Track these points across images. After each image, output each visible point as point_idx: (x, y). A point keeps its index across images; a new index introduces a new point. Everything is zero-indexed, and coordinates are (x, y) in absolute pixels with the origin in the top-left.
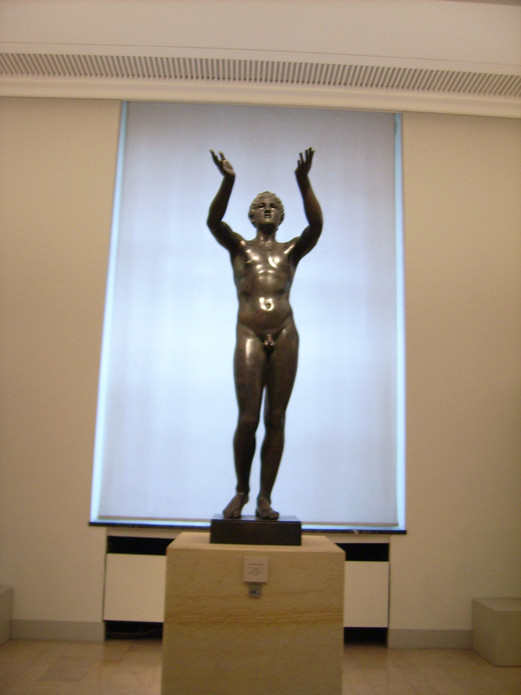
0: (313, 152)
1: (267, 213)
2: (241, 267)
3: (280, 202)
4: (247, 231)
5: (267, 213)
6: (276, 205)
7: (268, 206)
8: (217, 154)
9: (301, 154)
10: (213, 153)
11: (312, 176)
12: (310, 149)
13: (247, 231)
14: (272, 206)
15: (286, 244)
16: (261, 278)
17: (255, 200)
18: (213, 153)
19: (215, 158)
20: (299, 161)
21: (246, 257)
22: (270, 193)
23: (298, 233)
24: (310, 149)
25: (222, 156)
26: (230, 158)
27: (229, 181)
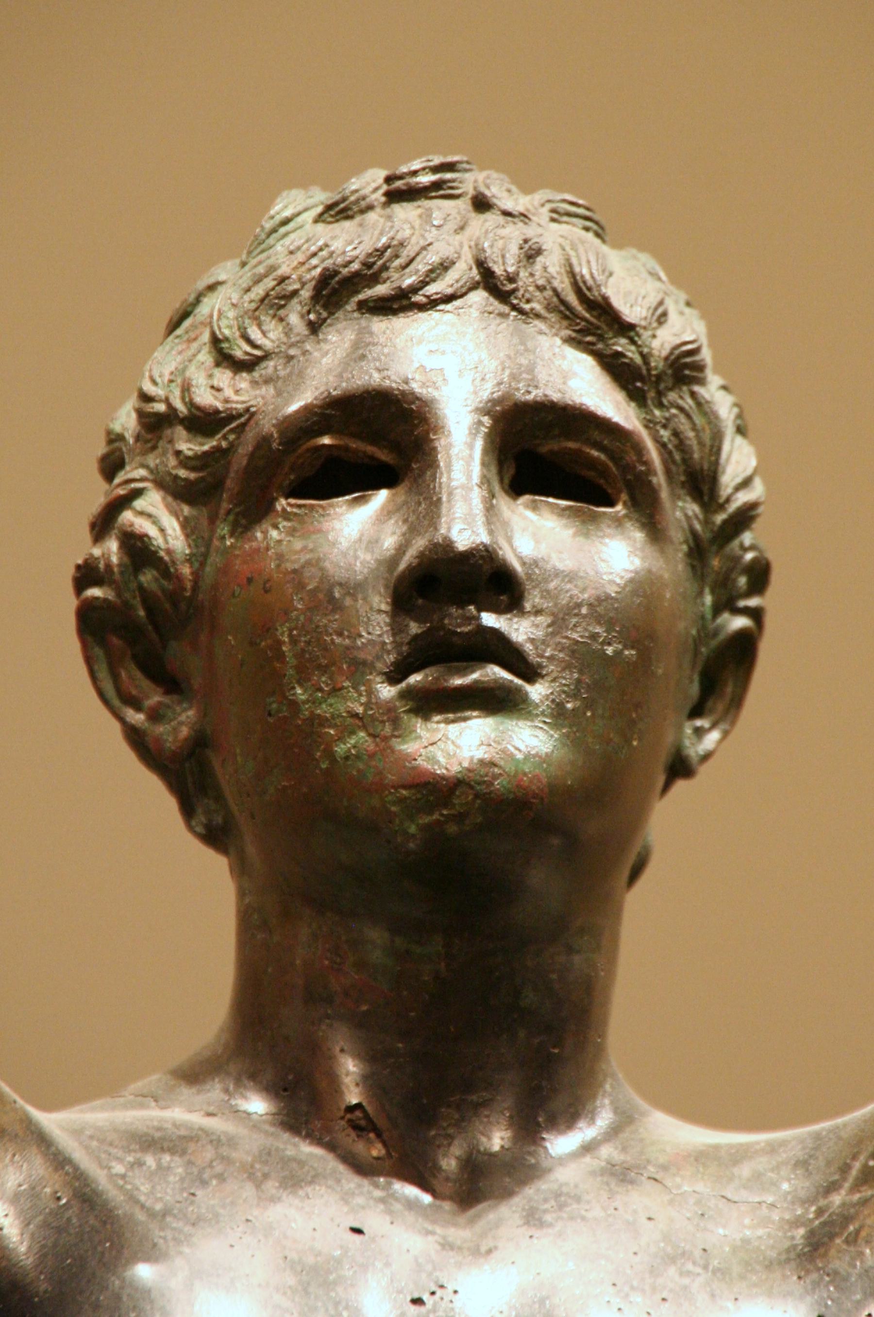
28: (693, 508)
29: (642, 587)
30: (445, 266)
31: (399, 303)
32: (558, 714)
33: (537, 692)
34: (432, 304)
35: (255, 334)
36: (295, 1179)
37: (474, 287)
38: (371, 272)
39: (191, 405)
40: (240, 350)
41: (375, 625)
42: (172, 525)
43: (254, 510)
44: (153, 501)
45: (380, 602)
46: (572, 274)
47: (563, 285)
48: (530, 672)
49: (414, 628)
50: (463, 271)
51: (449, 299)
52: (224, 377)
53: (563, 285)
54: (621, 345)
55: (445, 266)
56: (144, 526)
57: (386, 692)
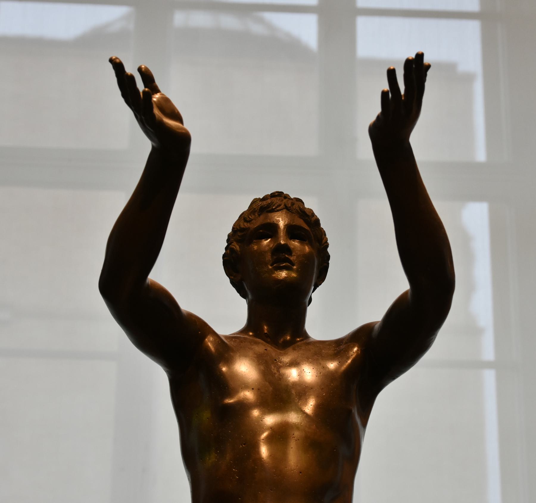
0: (428, 67)
1: (277, 253)
2: (206, 416)
3: (317, 222)
4: (221, 308)
5: (277, 253)
6: (308, 228)
7: (282, 234)
8: (130, 69)
9: (391, 74)
10: (118, 67)
11: (424, 141)
12: (420, 56)
13: (221, 308)
14: (292, 231)
15: (338, 342)
16: (264, 451)
17: (243, 217)
18: (118, 67)
19: (125, 82)
20: (384, 94)
21: (224, 386)
22: (286, 197)
23: (375, 313)
24: (420, 56)
25: (147, 77)
26: (173, 87)
27: (170, 153)
28: (318, 244)
29: (310, 253)
30: (280, 205)
31: (273, 211)
32: (297, 271)
33: (295, 267)
34: (278, 211)
35: (250, 217)
36: (256, 343)
37: (284, 209)
38: (269, 206)
39: (240, 228)
40: (248, 219)
41: (269, 257)
42: (238, 247)
43: (250, 242)
44: (235, 243)
45: (269, 254)
46: (299, 207)
47: (298, 209)
48: (293, 265)
49: (275, 257)
50: (282, 206)
51: (280, 210)
52: (245, 224)
53: (298, 209)
54: (307, 218)
55: (280, 205)
56: (233, 247)
57: (270, 267)
